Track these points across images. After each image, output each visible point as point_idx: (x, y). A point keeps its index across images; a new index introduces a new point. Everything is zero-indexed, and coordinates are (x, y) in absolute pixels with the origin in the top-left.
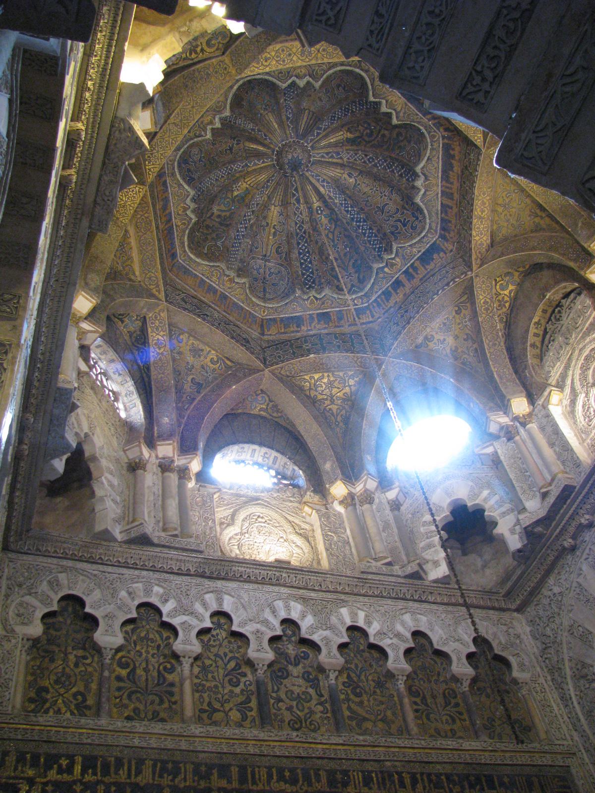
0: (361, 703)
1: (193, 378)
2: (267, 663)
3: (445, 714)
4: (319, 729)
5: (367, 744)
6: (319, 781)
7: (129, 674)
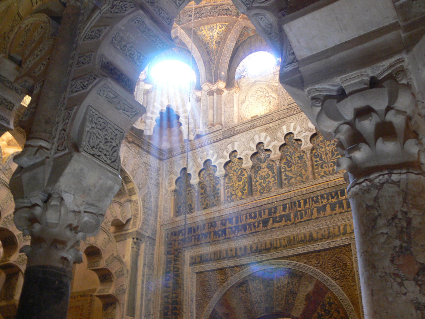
0: (290, 171)
1: (216, 41)
2: (250, 167)
3: (332, 162)
4: (271, 189)
5: (285, 192)
6: (264, 214)
7: (204, 191)
